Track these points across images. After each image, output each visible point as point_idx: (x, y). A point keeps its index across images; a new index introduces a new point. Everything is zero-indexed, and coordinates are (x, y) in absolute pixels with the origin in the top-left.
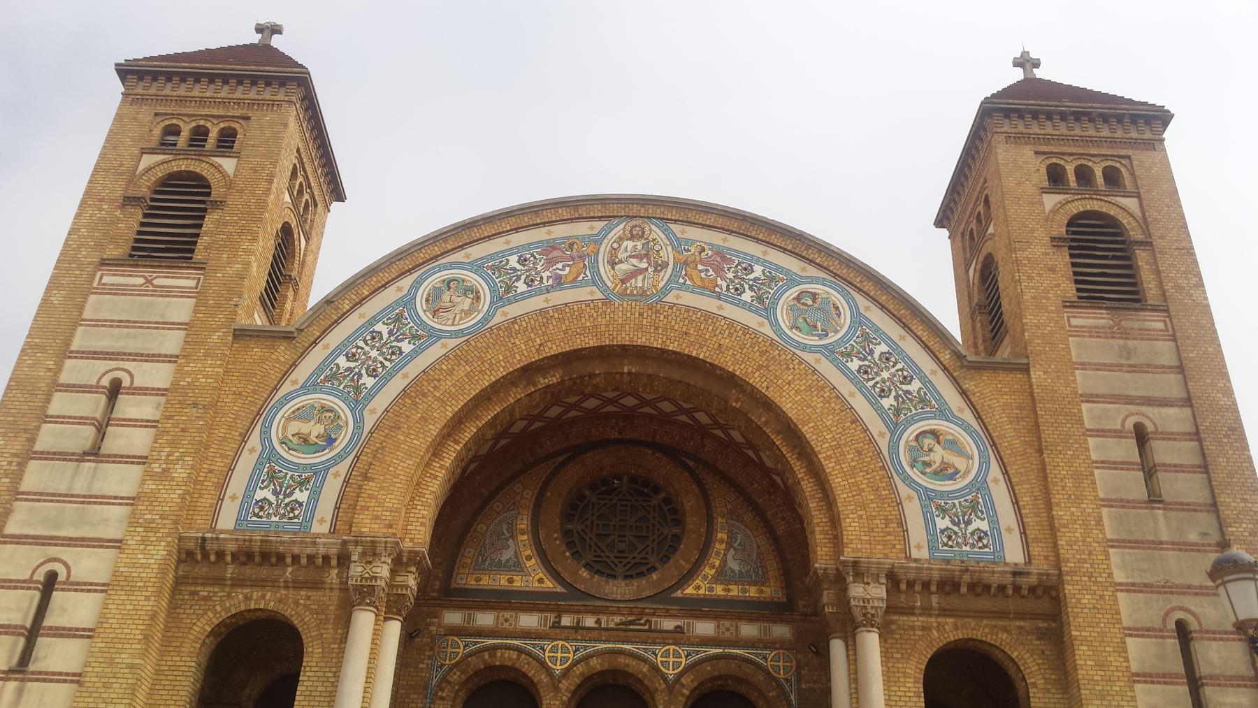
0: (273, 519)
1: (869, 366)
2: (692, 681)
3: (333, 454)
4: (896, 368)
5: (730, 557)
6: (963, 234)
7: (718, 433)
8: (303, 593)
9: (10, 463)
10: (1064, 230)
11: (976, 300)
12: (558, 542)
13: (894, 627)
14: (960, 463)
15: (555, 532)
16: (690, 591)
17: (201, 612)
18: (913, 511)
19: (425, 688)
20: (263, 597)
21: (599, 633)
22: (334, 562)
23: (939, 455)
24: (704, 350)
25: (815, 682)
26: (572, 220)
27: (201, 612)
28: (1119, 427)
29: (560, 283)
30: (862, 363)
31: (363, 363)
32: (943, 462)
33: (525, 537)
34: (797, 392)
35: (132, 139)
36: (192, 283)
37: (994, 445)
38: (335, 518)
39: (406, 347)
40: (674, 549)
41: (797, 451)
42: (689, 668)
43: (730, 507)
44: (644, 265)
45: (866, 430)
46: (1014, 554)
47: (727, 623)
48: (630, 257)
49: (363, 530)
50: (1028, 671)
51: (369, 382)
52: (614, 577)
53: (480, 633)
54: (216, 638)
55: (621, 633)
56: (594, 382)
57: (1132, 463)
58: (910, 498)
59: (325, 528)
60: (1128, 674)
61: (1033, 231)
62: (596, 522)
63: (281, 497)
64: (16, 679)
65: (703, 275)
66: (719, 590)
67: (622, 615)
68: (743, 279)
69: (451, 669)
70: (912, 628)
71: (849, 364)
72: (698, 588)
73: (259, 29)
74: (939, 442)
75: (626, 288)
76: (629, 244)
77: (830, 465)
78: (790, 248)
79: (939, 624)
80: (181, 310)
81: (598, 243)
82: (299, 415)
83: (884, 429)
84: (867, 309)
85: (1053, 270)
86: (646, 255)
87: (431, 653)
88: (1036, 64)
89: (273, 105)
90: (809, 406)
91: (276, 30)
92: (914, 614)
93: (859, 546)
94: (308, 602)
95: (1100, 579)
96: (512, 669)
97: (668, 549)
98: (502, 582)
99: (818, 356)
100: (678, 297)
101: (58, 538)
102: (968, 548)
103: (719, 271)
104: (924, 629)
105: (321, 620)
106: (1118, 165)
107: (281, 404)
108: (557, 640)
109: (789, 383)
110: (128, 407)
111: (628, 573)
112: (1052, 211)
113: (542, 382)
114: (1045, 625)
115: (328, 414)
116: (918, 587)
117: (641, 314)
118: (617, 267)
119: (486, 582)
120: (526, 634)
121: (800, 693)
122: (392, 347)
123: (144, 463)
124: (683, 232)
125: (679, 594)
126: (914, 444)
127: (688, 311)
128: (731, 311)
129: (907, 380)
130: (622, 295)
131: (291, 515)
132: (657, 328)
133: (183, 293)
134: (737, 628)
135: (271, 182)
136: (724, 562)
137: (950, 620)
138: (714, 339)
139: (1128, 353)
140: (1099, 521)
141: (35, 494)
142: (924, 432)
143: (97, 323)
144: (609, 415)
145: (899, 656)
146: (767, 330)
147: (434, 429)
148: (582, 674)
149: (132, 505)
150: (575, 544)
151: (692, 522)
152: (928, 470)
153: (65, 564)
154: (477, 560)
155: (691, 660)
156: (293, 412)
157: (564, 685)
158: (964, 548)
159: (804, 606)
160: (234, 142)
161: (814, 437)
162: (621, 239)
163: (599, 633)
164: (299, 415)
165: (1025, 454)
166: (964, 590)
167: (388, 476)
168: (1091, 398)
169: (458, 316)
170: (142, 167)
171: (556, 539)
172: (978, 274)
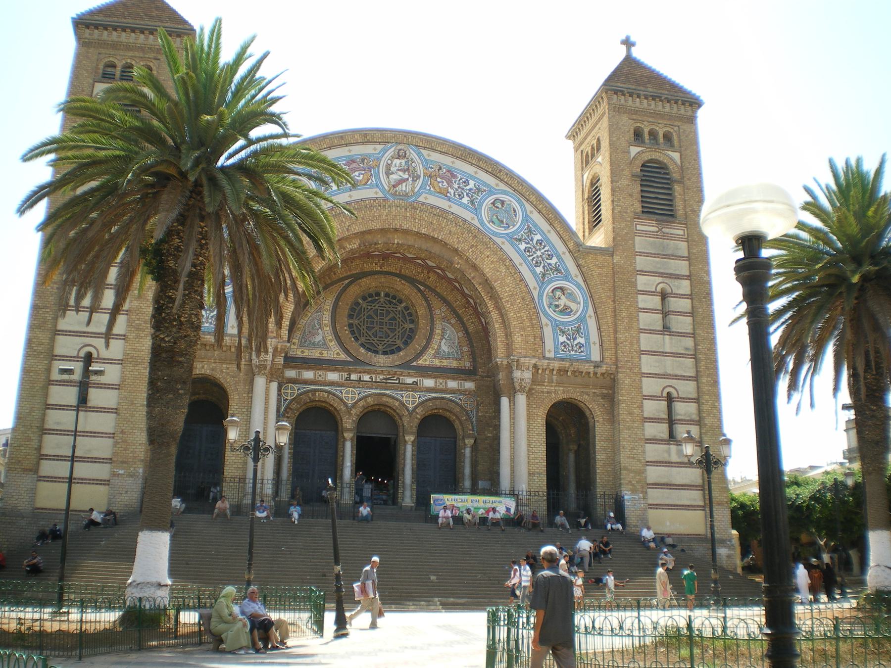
6: (582, 151)
8: (224, 366)
10: (639, 170)
11: (586, 196)
14: (573, 306)
16: (421, 362)
18: (548, 332)
20: (203, 367)
21: (372, 384)
23: (563, 301)
25: (486, 412)
26: (363, 143)
32: (565, 305)
33: (328, 328)
34: (492, 262)
35: (87, 71)
37: (591, 297)
42: (420, 404)
43: (443, 314)
44: (406, 176)
45: (527, 286)
46: (596, 356)
47: (441, 381)
48: (398, 170)
53: (306, 382)
55: (384, 384)
57: (658, 310)
58: (547, 325)
61: (623, 170)
62: (366, 319)
65: (440, 185)
66: (437, 362)
67: (384, 374)
68: (463, 189)
70: (543, 392)
71: (520, 246)
72: (426, 360)
74: (564, 294)
76: (397, 162)
78: (490, 171)
81: (379, 160)
83: (537, 286)
85: (631, 195)
86: (408, 170)
88: (633, 44)
90: (498, 271)
96: (325, 402)
97: (409, 338)
98: (315, 354)
99: (504, 240)
100: (426, 198)
101: (88, 333)
102: (573, 353)
106: (672, 131)
109: (488, 257)
112: (634, 157)
114: (606, 392)
116: (547, 372)
118: (391, 176)
119: (307, 354)
120: (332, 384)
121: (478, 418)
125: (414, 364)
126: (551, 294)
128: (456, 209)
129: (550, 257)
130: (395, 194)
132: (415, 219)
136: (440, 346)
137: (561, 388)
139: (664, 248)
142: (557, 288)
146: (476, 222)
148: (363, 406)
150: (355, 332)
151: (422, 322)
155: (421, 400)
157: (353, 411)
162: (393, 157)
163: (372, 384)
166: (569, 374)
168: (643, 272)
172: (589, 181)
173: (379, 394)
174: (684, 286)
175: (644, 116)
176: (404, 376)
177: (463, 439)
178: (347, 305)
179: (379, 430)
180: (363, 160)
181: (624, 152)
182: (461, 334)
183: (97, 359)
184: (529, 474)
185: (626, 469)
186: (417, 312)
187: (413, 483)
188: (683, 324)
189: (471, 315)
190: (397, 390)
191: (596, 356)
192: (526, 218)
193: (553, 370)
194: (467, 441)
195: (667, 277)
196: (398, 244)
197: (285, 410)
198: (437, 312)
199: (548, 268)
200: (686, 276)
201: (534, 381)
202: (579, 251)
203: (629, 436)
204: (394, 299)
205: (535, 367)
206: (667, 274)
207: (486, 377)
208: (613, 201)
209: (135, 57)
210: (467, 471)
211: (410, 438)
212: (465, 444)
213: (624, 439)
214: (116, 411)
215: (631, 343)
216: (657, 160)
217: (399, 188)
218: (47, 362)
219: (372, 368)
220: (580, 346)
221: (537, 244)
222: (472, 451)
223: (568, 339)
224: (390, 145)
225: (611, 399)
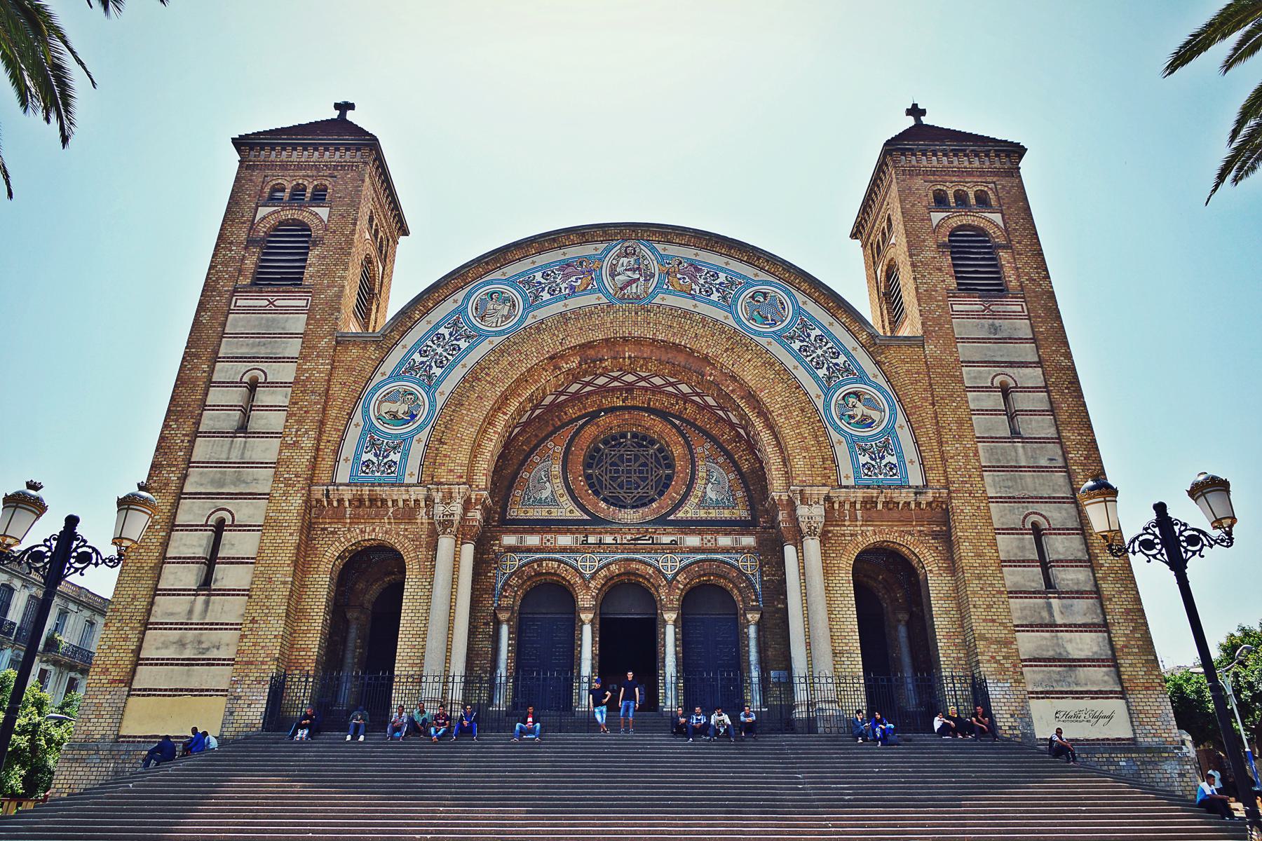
0: (376, 474)
1: (807, 346)
2: (685, 579)
3: (415, 425)
4: (827, 346)
5: (708, 489)
6: (872, 244)
7: (697, 399)
9: (182, 441)
10: (946, 239)
12: (582, 483)
13: (830, 535)
14: (875, 415)
15: (580, 476)
16: (680, 515)
17: (330, 542)
18: (842, 452)
19: (494, 590)
20: (374, 530)
21: (614, 549)
22: (422, 504)
23: (860, 410)
24: (685, 338)
25: (774, 575)
27: (330, 542)
28: (990, 385)
29: (574, 292)
30: (802, 344)
31: (432, 358)
33: (558, 481)
36: (303, 303)
38: (421, 473)
39: (463, 344)
40: (667, 486)
41: (756, 411)
43: (707, 453)
45: (806, 394)
46: (916, 479)
47: (709, 537)
48: (626, 270)
49: (442, 480)
50: (926, 562)
51: (437, 371)
52: (625, 507)
53: (529, 550)
54: (342, 560)
55: (633, 547)
56: (603, 365)
59: (414, 480)
60: (999, 561)
61: (924, 241)
63: (381, 458)
64: (203, 595)
66: (702, 514)
69: (511, 577)
70: (844, 535)
72: (689, 511)
73: (337, 106)
74: (859, 401)
75: (624, 294)
76: (625, 260)
77: (782, 421)
78: (745, 259)
79: (862, 531)
80: (298, 323)
81: (601, 260)
82: (390, 398)
84: (805, 303)
85: (940, 270)
86: (638, 269)
87: (496, 566)
88: (923, 112)
89: (352, 166)
90: (764, 377)
91: (351, 106)
92: (844, 526)
93: (804, 479)
94: (406, 533)
95: (976, 495)
96: (555, 574)
98: (540, 513)
100: (663, 299)
101: (223, 494)
102: (882, 477)
103: (694, 279)
104: (852, 535)
105: (416, 545)
106: (986, 189)
107: (376, 389)
108: (586, 553)
110: (264, 397)
111: (635, 504)
112: (937, 225)
113: (565, 366)
114: (938, 529)
115: (410, 397)
116: (847, 506)
117: (636, 313)
118: (616, 278)
120: (563, 550)
121: (763, 583)
122: (452, 345)
123: (280, 437)
124: (665, 249)
125: (672, 517)
126: (842, 402)
127: (671, 309)
128: (704, 309)
129: (836, 355)
130: (623, 298)
131: (389, 471)
132: (649, 323)
133: (297, 310)
134: (716, 540)
135: (355, 224)
137: (870, 528)
138: (692, 330)
140: (976, 453)
141: (203, 463)
142: (850, 393)
143: (236, 335)
144: (614, 389)
145: (834, 555)
146: (731, 322)
147: (488, 404)
148: (605, 576)
149: (274, 468)
150: (595, 486)
151: (679, 465)
152: (852, 421)
153: (230, 512)
154: (524, 498)
155: (683, 564)
156: (385, 396)
158: (880, 477)
159: (764, 522)
160: (325, 195)
161: (769, 400)
163: (614, 549)
164: (390, 398)
165: (922, 406)
166: (880, 506)
167: (456, 441)
169: (500, 320)
170: (258, 218)
171: (581, 481)
172: (884, 274)
173: (627, 560)
174: (1033, 376)
175: (945, 175)
176: (659, 534)
177: (745, 615)
178: (582, 450)
179: (630, 610)
180: (581, 263)
181: (923, 220)
182: (732, 476)
183: (230, 526)
184: (835, 654)
185: (983, 637)
186: (672, 453)
187: (678, 678)
188: (1041, 427)
189: (743, 451)
190: (649, 552)
191: (916, 479)
192: (799, 311)
193: (855, 502)
194: (749, 616)
195: (1007, 367)
196: (630, 357)
197: (503, 588)
198: (699, 450)
199: (834, 370)
200: (1034, 363)
201: (829, 517)
202: (875, 344)
203: (982, 589)
204: (643, 440)
205: (828, 498)
206: (1006, 362)
207: (769, 528)
208: (915, 279)
209: (308, 176)
210: (753, 656)
211: (670, 617)
212: (748, 622)
213: (974, 593)
214: (247, 593)
215: (966, 456)
216: (970, 225)
217: (627, 291)
218: (164, 534)
219: (615, 527)
220: (892, 466)
221: (815, 340)
222: (758, 631)
223: (872, 459)
224: (615, 242)
225: (946, 540)
